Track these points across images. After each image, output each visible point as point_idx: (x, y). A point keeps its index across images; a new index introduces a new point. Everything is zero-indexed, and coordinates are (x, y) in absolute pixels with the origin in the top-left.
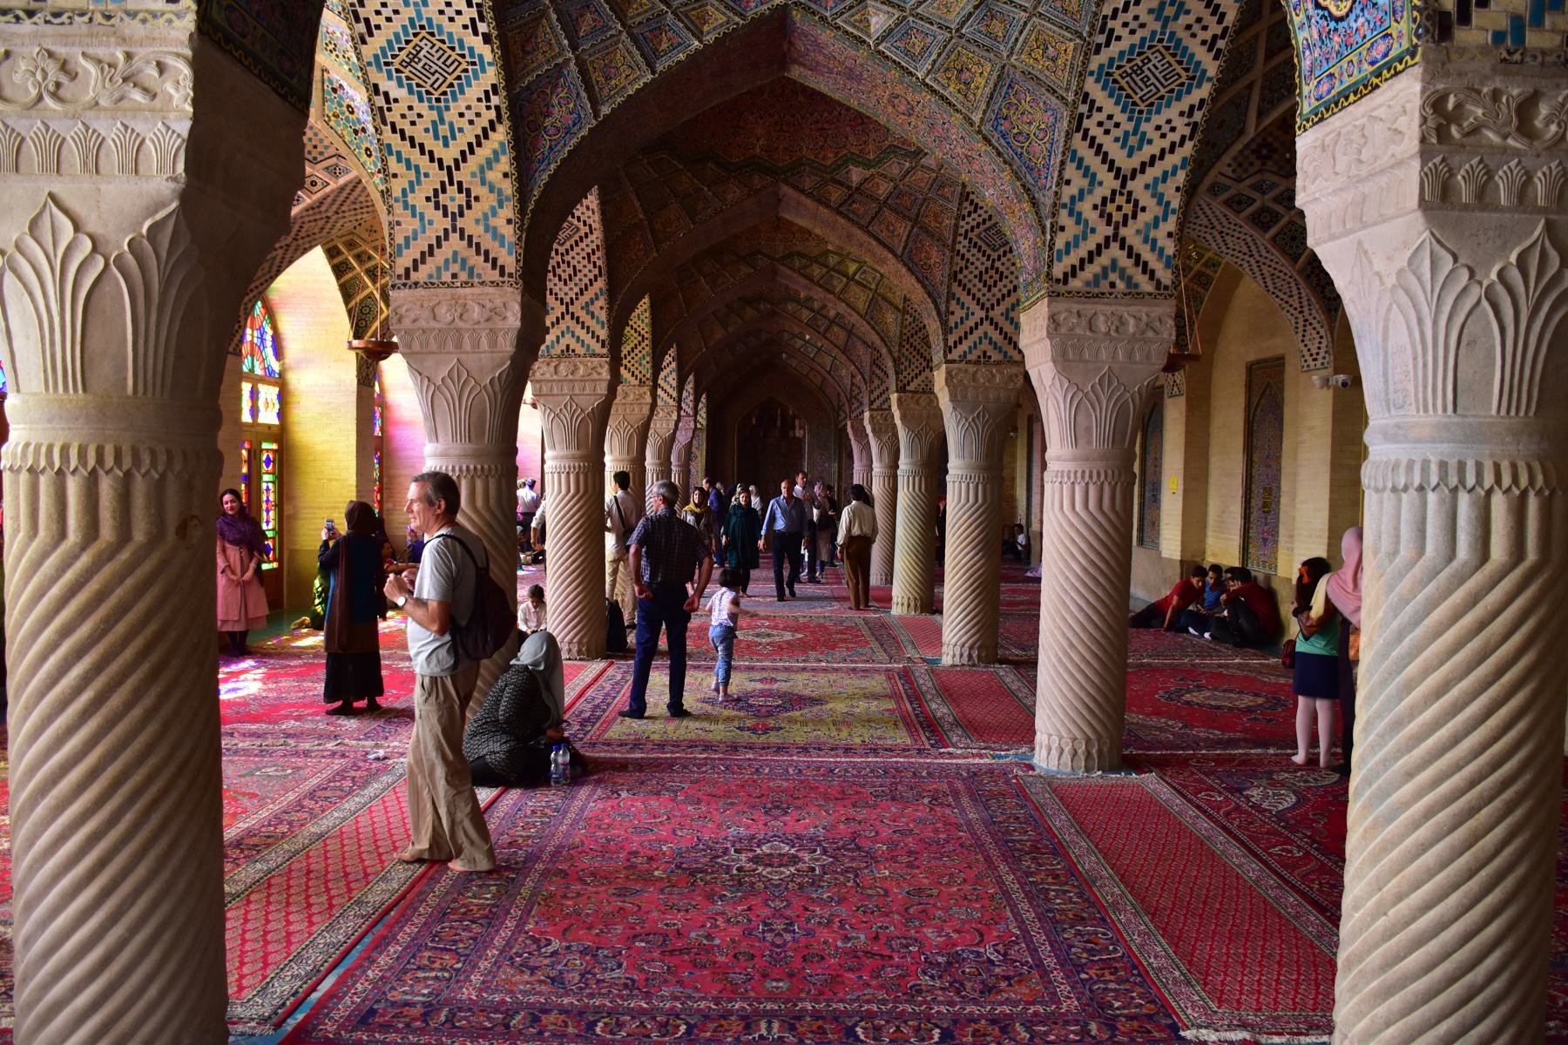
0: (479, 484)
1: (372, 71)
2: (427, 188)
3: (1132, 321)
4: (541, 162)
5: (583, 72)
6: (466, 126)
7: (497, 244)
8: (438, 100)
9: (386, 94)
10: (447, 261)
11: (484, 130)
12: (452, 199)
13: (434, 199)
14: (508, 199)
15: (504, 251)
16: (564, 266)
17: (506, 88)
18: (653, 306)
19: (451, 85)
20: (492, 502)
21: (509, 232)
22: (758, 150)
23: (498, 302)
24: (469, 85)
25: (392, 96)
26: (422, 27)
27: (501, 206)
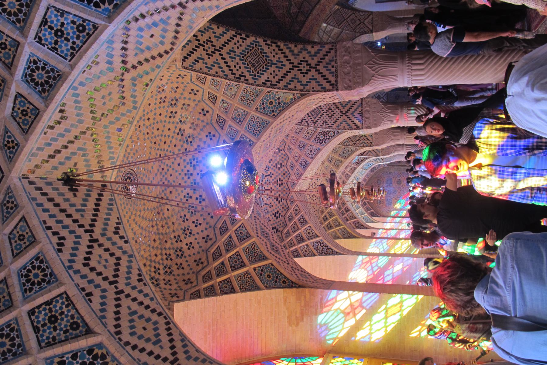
1: (258, 82)
2: (300, 76)
7: (321, 52)
8: (268, 63)
9: (266, 81)
10: (327, 70)
11: (279, 50)
12: (304, 67)
13: (305, 74)
14: (304, 47)
15: (324, 49)
19: (263, 56)
21: (316, 48)
23: (343, 50)
24: (263, 50)
27: (307, 50)
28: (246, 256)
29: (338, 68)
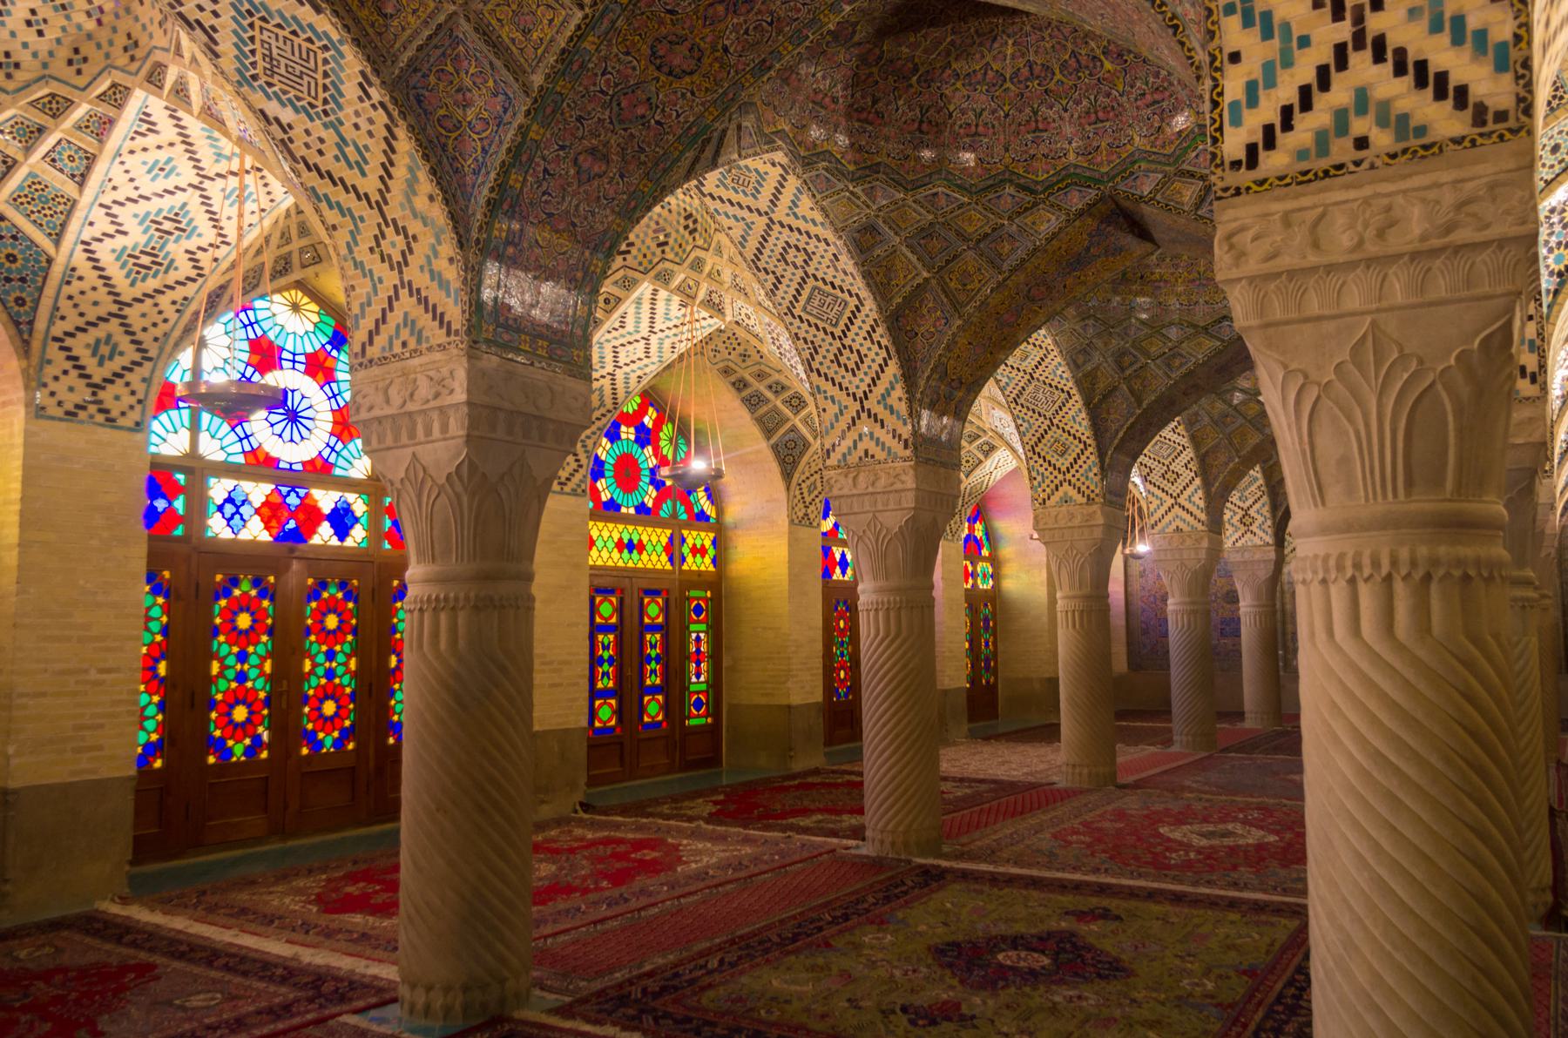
0: (443, 617)
3: (1416, 211)
4: (476, 173)
5: (484, 32)
6: (369, 142)
9: (277, 120)
12: (394, 244)
14: (443, 232)
15: (451, 301)
16: (846, 352)
17: (377, 72)
18: (1088, 404)
19: (325, 88)
20: (462, 644)
22: (1072, 157)
23: (445, 371)
25: (284, 121)
26: (248, 11)
28: (21, 188)
29: (399, 365)
